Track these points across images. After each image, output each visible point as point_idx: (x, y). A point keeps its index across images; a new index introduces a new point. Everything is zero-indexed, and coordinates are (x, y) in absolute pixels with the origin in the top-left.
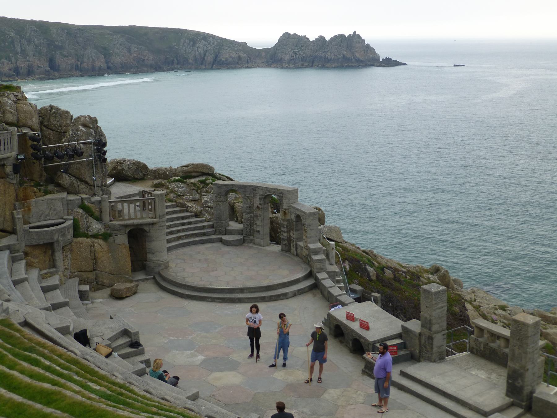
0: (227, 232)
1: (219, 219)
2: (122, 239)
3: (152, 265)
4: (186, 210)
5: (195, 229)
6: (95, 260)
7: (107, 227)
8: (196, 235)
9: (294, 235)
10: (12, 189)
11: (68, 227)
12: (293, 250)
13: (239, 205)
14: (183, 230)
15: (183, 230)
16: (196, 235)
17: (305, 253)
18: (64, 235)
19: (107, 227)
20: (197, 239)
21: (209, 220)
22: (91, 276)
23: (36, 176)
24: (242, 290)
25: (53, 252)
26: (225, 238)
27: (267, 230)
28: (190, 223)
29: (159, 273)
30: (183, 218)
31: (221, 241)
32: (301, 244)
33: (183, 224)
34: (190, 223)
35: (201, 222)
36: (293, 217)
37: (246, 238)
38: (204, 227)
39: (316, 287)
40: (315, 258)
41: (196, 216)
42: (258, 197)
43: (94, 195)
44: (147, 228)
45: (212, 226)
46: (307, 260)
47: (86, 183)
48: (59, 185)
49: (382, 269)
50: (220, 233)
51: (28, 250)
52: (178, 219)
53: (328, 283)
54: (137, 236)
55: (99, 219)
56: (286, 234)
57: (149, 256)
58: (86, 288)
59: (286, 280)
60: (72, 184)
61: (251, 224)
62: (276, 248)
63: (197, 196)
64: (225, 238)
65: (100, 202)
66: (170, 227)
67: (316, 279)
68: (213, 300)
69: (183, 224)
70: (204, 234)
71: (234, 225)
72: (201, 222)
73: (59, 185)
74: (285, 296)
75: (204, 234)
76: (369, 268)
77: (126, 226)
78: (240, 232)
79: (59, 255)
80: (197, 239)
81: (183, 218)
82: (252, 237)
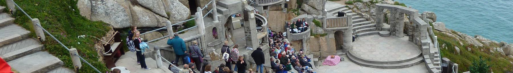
0: (382, 30)
1: (379, 23)
2: (332, 36)
3: (345, 48)
4: (362, 17)
5: (366, 27)
6: (320, 47)
7: (325, 30)
8: (367, 31)
9: (416, 34)
10: (284, 15)
11: (308, 32)
12: (414, 41)
13: (389, 15)
14: (360, 28)
15: (360, 28)
16: (367, 31)
17: (420, 44)
18: (307, 36)
19: (325, 30)
20: (367, 33)
21: (374, 23)
22: (318, 53)
23: (293, 7)
24: (387, 63)
25: (302, 43)
26: (381, 32)
27: (402, 30)
28: (364, 24)
29: (348, 52)
30: (360, 21)
31: (379, 34)
32: (418, 39)
33: (360, 25)
34: (364, 24)
35: (369, 23)
36: (415, 25)
37: (392, 33)
38: (370, 27)
39: (423, 61)
40: (424, 47)
41: (367, 20)
42: (398, 13)
43: (319, 14)
44: (343, 31)
45: (375, 26)
46: (420, 46)
47: (315, 9)
48: (303, 10)
49: (466, 48)
50: (379, 30)
51: (292, 43)
52: (358, 22)
53: (428, 61)
54: (339, 35)
55: (322, 27)
56: (411, 33)
57: (344, 44)
58: (317, 60)
59: (408, 58)
60: (309, 10)
61: (395, 26)
62: (407, 38)
63: (367, 10)
64: (381, 32)
65: (322, 19)
66: (354, 26)
67: (424, 58)
68: (373, 67)
69: (360, 25)
70: (371, 30)
71: (386, 26)
72: (369, 23)
73: (303, 10)
74: (407, 66)
75: (371, 30)
76: (457, 48)
77: (334, 30)
78: (389, 30)
79: (305, 45)
80: (367, 33)
81: (360, 21)
82: (394, 33)
